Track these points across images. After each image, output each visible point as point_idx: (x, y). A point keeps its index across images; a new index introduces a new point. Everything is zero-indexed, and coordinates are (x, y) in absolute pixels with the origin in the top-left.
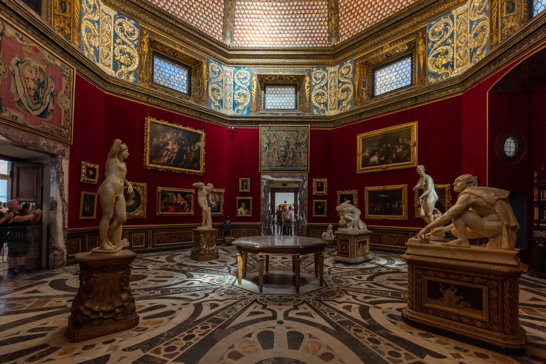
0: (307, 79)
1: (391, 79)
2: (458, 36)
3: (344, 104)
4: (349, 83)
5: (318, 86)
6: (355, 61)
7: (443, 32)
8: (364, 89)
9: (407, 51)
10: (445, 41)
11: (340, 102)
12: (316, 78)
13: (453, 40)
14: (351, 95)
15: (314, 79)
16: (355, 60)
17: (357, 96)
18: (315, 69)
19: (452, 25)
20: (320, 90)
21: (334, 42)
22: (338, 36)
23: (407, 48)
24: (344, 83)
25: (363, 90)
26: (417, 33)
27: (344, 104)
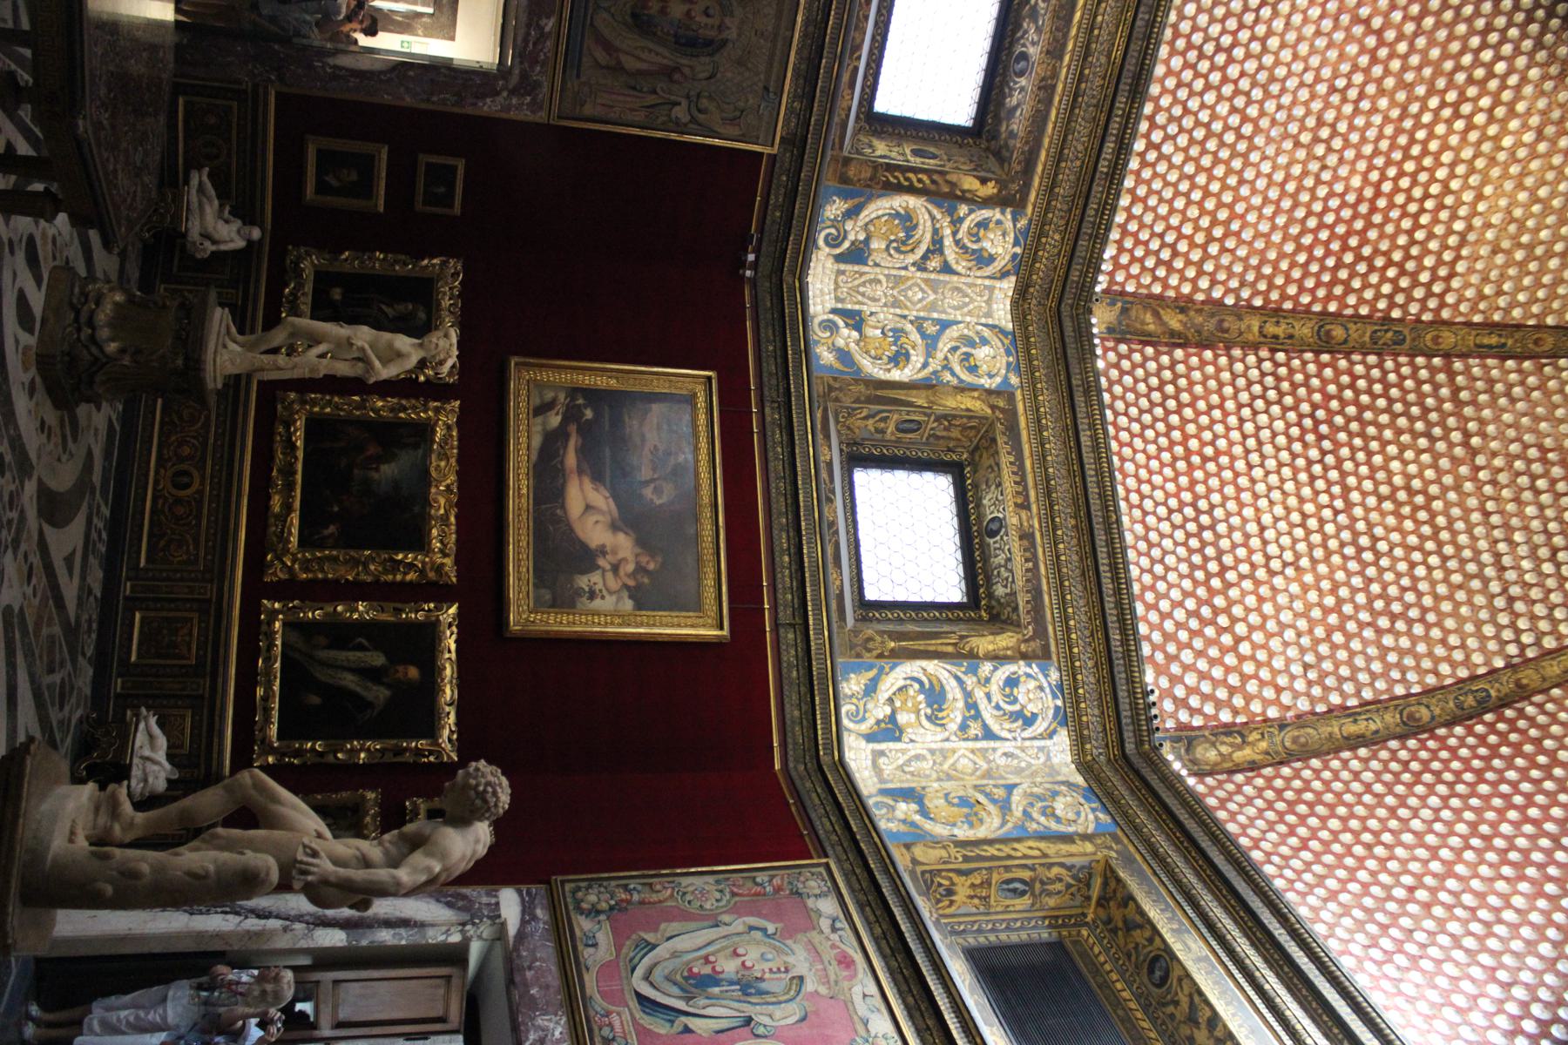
0: (990, 189)
1: (904, 535)
2: (984, 751)
3: (846, 336)
4: (925, 365)
6: (1005, 392)
7: (1017, 707)
9: (990, 595)
10: (978, 716)
11: (856, 320)
12: (983, 224)
13: (976, 738)
14: (875, 370)
15: (985, 213)
16: (1011, 397)
18: (1022, 223)
19: (1026, 734)
20: (928, 236)
21: (1099, 320)
22: (1118, 333)
23: (1000, 591)
24: (931, 343)
25: (884, 419)
26: (1041, 632)
27: (845, 332)
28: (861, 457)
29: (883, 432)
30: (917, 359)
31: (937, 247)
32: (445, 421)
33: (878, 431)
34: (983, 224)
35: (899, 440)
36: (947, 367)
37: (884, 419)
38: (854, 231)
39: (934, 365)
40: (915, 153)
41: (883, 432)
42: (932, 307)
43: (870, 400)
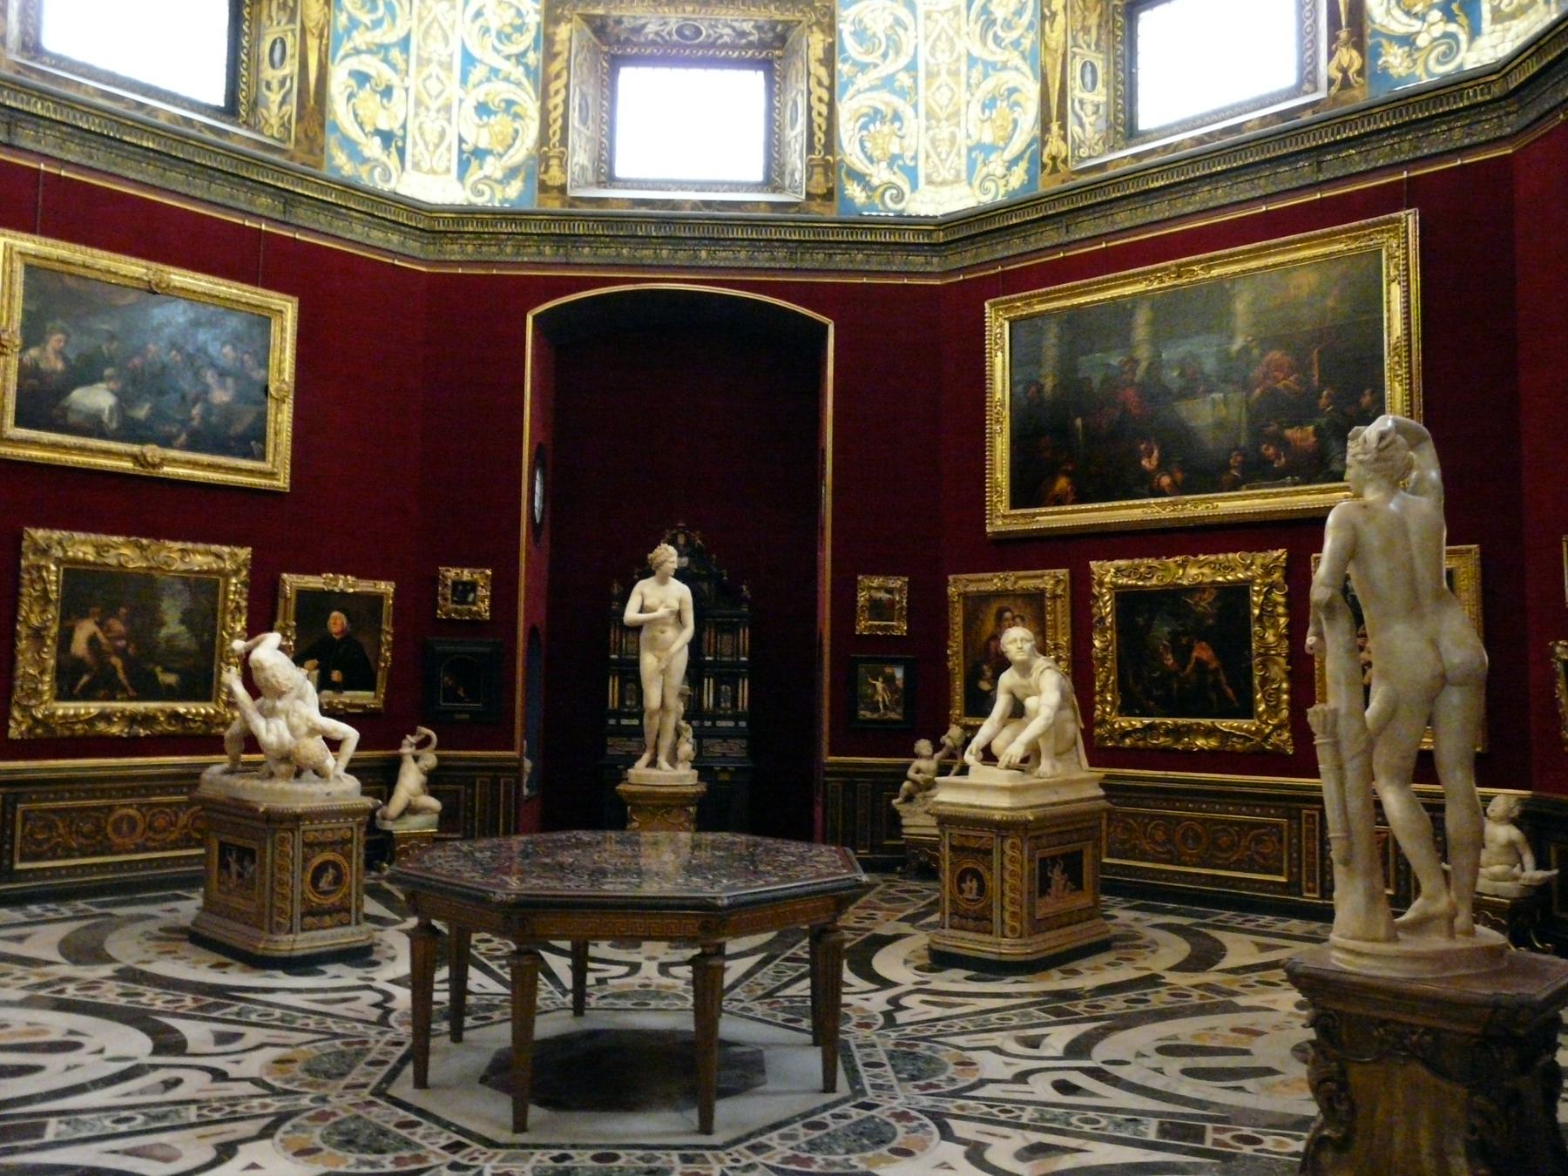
5: (873, 75)
8: (1087, 96)
17: (1055, 127)
24: (990, 67)
28: (1125, 127)
29: (1097, 106)
30: (1010, 79)
31: (887, 83)
32: (1108, 573)
33: (1096, 112)
34: (860, 34)
35: (1107, 84)
36: (1016, 44)
37: (1081, 102)
38: (880, 175)
39: (1015, 58)
40: (794, 122)
41: (1097, 106)
42: (954, 73)
43: (1063, 127)
